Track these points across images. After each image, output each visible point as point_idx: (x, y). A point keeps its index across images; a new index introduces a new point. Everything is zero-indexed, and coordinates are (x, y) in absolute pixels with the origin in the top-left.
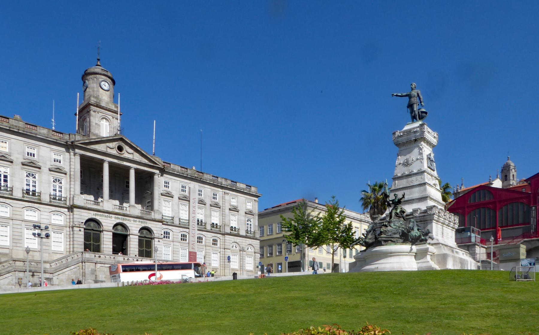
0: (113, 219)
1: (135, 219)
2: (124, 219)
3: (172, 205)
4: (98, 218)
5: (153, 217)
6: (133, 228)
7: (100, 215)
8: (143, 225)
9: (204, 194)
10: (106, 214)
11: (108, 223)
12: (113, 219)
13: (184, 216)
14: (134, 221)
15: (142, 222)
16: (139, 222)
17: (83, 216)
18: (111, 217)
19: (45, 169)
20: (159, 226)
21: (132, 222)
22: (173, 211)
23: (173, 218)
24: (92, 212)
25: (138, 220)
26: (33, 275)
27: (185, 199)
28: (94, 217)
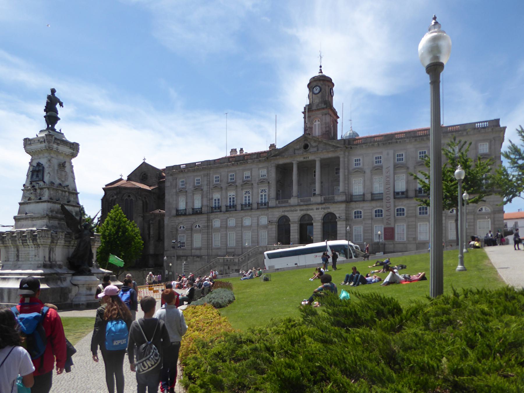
0: (298, 211)
1: (318, 207)
2: (307, 210)
3: (364, 181)
4: (286, 214)
5: (336, 201)
6: (316, 216)
7: (288, 211)
8: (326, 211)
9: (406, 157)
10: (293, 209)
11: (294, 216)
12: (298, 211)
13: (378, 187)
14: (317, 209)
15: (324, 209)
16: (322, 208)
17: (277, 214)
18: (297, 211)
19: (255, 185)
20: (341, 209)
21: (315, 210)
22: (364, 187)
23: (364, 195)
24: (281, 210)
25: (320, 207)
26: (229, 268)
27: (378, 169)
28: (283, 214)
